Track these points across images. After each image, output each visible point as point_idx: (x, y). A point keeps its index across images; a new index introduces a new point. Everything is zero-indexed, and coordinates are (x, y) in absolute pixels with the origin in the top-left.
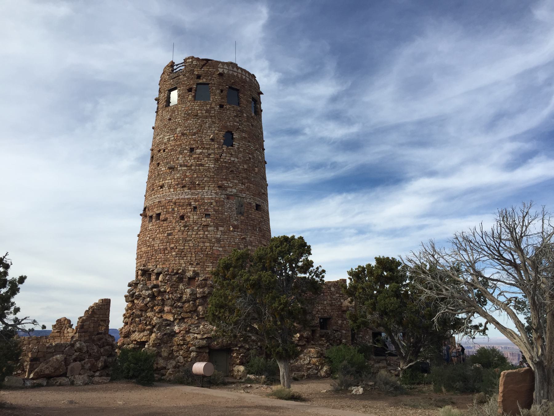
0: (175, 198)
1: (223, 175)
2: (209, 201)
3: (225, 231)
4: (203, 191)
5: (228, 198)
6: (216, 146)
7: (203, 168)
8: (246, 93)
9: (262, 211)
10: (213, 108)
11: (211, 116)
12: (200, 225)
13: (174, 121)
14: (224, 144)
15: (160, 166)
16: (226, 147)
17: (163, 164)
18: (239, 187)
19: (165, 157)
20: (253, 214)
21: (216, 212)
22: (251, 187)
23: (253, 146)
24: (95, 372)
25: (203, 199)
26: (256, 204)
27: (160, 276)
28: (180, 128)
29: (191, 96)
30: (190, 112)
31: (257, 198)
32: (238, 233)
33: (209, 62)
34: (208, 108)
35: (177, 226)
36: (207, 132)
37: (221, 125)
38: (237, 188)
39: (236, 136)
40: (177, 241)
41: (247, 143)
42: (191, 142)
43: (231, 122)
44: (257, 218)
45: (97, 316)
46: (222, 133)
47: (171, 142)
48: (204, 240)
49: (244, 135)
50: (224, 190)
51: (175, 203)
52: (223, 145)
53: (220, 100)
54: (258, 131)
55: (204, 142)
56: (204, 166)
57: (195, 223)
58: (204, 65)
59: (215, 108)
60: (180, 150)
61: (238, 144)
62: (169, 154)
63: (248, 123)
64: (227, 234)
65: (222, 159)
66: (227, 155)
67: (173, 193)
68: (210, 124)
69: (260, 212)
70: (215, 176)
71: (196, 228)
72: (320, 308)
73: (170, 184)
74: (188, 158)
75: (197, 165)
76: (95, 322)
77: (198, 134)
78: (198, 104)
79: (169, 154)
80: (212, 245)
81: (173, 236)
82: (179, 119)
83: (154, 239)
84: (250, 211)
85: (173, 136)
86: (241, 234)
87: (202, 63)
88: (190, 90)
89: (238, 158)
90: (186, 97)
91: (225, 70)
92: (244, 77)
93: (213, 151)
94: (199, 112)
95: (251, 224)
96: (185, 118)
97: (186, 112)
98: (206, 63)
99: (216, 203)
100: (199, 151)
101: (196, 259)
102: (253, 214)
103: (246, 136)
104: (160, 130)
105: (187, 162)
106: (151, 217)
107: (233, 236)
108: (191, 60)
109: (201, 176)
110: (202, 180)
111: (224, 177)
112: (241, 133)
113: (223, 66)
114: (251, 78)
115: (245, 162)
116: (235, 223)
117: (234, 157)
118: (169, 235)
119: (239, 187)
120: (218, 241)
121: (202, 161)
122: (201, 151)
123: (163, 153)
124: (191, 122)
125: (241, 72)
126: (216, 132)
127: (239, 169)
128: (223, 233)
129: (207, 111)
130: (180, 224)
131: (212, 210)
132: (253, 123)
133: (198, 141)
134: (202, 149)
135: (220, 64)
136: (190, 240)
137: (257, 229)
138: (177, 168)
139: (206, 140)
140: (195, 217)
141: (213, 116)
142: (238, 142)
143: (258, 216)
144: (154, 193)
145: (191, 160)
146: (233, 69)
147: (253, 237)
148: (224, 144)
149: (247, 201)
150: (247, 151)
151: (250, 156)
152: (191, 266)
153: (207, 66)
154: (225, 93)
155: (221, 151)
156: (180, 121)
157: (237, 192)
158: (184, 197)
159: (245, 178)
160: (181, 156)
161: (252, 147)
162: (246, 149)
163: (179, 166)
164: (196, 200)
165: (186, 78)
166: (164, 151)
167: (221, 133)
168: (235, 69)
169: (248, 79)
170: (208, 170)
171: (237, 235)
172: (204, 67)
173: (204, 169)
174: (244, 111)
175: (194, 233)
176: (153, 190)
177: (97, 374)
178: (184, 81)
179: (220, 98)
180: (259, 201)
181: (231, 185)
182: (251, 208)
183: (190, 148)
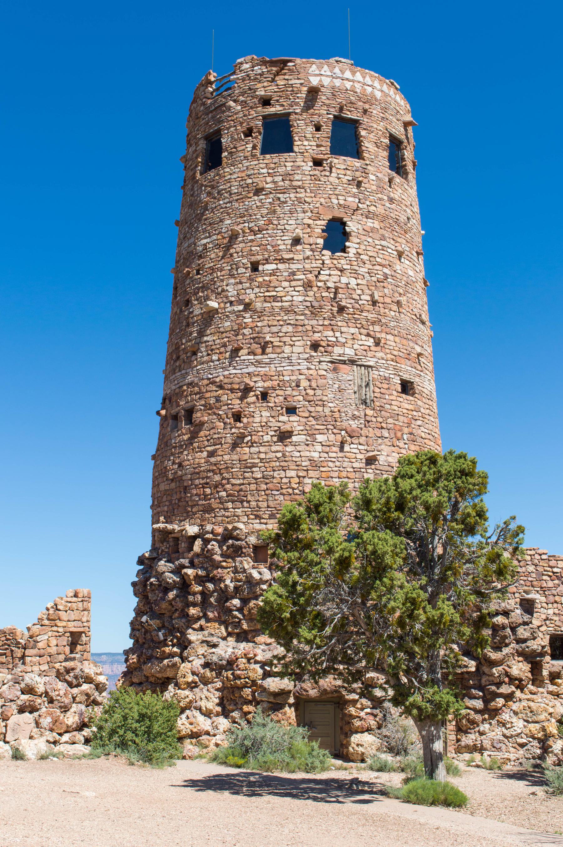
1: (324, 318)
2: (294, 378)
3: (331, 443)
4: (280, 356)
5: (335, 370)
6: (309, 253)
7: (279, 304)
8: (375, 126)
9: (416, 395)
12: (275, 431)
13: (217, 204)
14: (325, 247)
16: (330, 253)
18: (360, 343)
20: (393, 403)
21: (309, 401)
22: (388, 342)
23: (393, 248)
24: (60, 735)
26: (401, 380)
27: (196, 543)
30: (249, 181)
31: (403, 366)
32: (360, 447)
33: (290, 64)
35: (228, 435)
38: (356, 347)
39: (352, 226)
41: (377, 242)
42: (253, 249)
43: (340, 197)
44: (405, 411)
45: (64, 624)
48: (286, 464)
49: (372, 225)
50: (326, 352)
51: (221, 387)
52: (323, 249)
54: (405, 211)
55: (281, 247)
56: (282, 301)
57: (265, 426)
59: (304, 168)
61: (357, 246)
63: (380, 196)
64: (334, 449)
65: (320, 281)
66: (332, 273)
67: (218, 363)
68: (292, 205)
69: (411, 398)
70: (306, 322)
71: (267, 438)
72: (551, 612)
73: (210, 343)
74: (248, 285)
76: (60, 636)
77: (267, 229)
78: (265, 161)
80: (301, 474)
81: (219, 458)
84: (387, 397)
86: (366, 447)
88: (249, 133)
89: (356, 279)
90: (239, 149)
91: (323, 78)
92: (369, 89)
93: (300, 266)
94: (269, 179)
95: (391, 426)
98: (282, 69)
99: (309, 380)
101: (268, 507)
102: (393, 403)
103: (377, 225)
106: (175, 418)
107: (348, 454)
109: (275, 323)
110: (278, 333)
111: (326, 322)
112: (365, 220)
114: (387, 91)
116: (354, 424)
117: (349, 275)
118: (212, 454)
119: (360, 343)
121: (276, 289)
122: (273, 266)
125: (361, 79)
127: (360, 302)
129: (287, 176)
130: (233, 430)
131: (301, 398)
132: (392, 195)
134: (275, 262)
135: (314, 66)
136: (254, 465)
137: (405, 437)
139: (284, 243)
140: (265, 414)
142: (358, 241)
143: (407, 406)
144: (180, 366)
145: (253, 289)
146: (342, 72)
147: (394, 454)
148: (325, 247)
149: (381, 373)
150: (378, 260)
151: (386, 270)
152: (258, 521)
153: (285, 74)
154: (327, 129)
155: (315, 265)
157: (356, 355)
158: (239, 371)
159: (373, 323)
160: (232, 281)
161: (390, 250)
162: (375, 254)
163: (228, 305)
164: (266, 377)
165: (239, 108)
167: (319, 222)
168: (348, 74)
169: (378, 95)
171: (358, 451)
172: (277, 78)
173: (282, 308)
174: (369, 167)
175: (262, 449)
177: (66, 737)
178: (236, 114)
179: (315, 144)
181: (344, 340)
182: (389, 388)
183: (251, 263)
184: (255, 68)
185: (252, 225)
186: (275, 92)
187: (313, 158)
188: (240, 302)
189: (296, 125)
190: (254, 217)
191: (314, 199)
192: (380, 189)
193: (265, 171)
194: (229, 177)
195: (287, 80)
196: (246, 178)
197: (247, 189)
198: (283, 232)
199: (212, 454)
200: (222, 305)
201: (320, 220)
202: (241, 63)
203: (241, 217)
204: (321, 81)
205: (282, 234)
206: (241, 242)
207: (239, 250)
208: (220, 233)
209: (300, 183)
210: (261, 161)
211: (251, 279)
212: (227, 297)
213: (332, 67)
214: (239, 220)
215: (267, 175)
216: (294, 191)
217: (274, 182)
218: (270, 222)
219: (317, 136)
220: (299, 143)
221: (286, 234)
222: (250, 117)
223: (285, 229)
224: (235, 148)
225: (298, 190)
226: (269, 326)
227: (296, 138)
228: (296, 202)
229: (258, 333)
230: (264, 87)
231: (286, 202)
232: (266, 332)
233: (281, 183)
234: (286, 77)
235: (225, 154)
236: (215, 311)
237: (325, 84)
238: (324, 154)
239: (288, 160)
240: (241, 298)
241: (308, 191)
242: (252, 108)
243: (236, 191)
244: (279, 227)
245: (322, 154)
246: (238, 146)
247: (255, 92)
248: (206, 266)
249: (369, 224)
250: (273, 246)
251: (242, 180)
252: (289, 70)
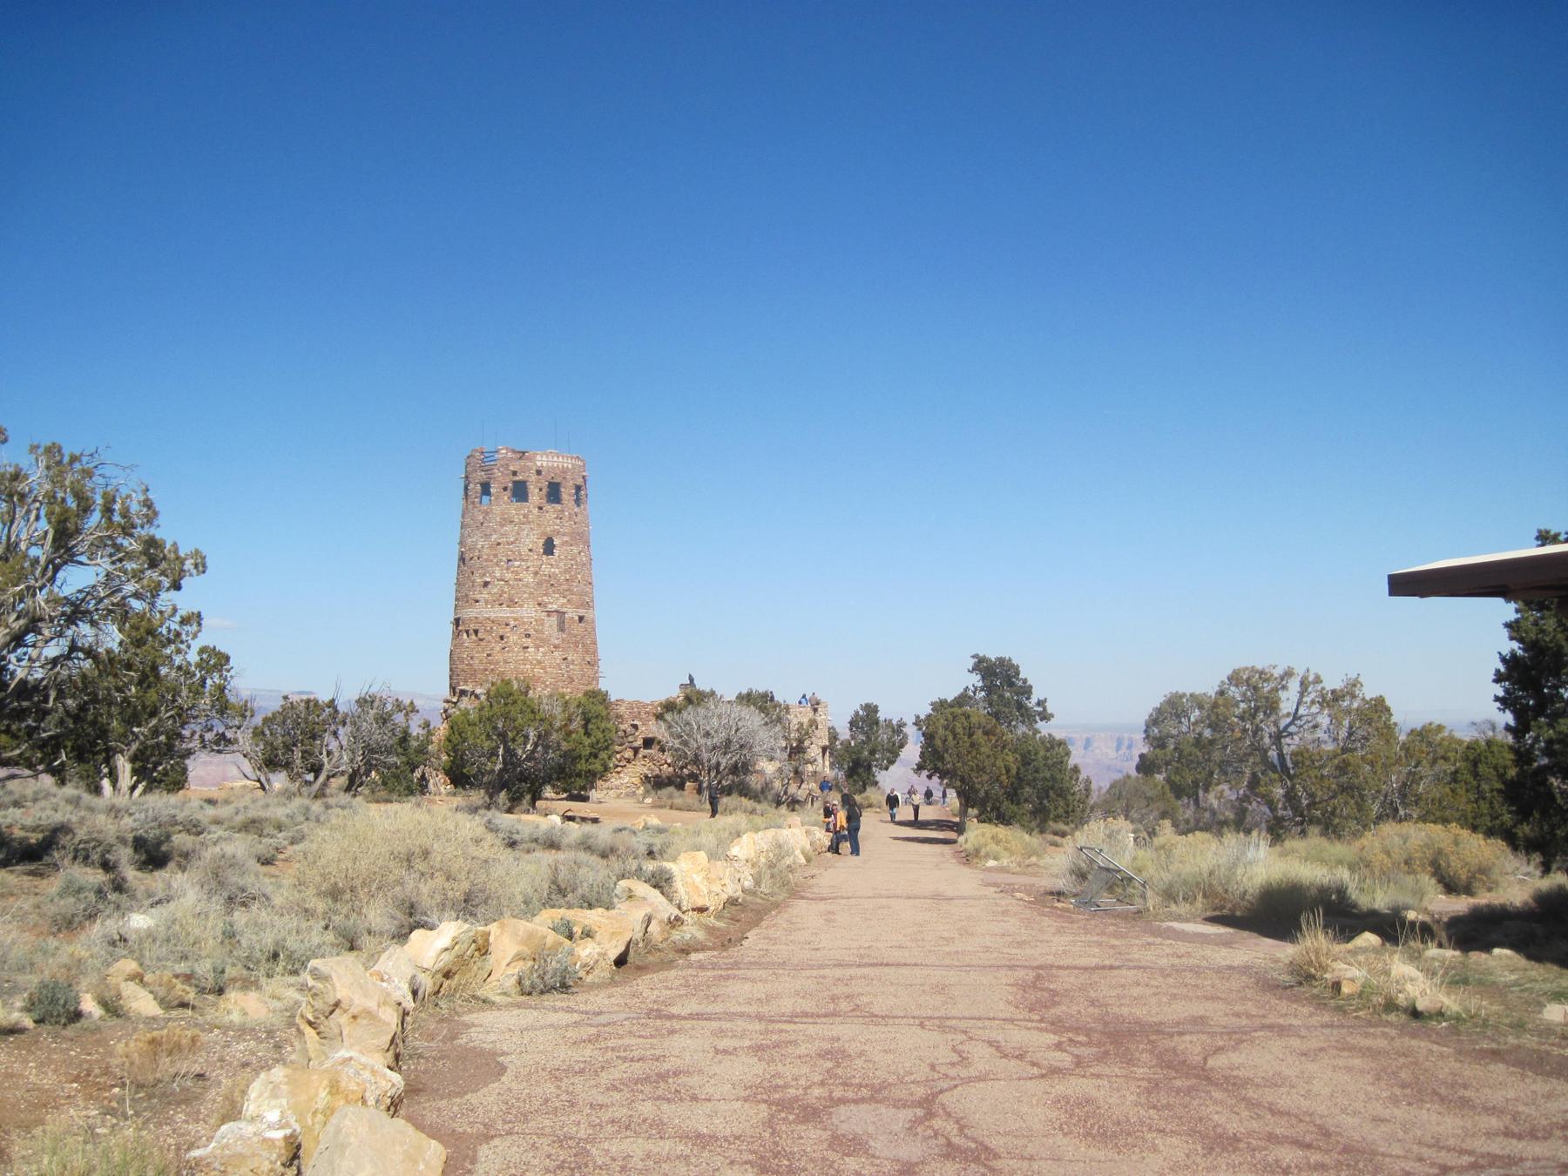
0: (493, 615)
5: (548, 616)
25: (522, 618)
39: (556, 542)
40: (498, 663)
46: (542, 542)
51: (493, 622)
57: (515, 644)
58: (520, 458)
75: (516, 580)
83: (472, 658)
88: (505, 489)
92: (565, 465)
100: (517, 563)
115: (566, 571)
118: (489, 655)
120: (539, 662)
128: (544, 654)
129: (525, 516)
139: (524, 550)
154: (545, 490)
164: (515, 619)
168: (555, 459)
169: (570, 466)
170: (527, 586)
176: (467, 602)
180: (582, 612)
188: (503, 580)
192: (570, 518)
199: (489, 655)
211: (508, 569)
213: (547, 457)
242: (507, 475)
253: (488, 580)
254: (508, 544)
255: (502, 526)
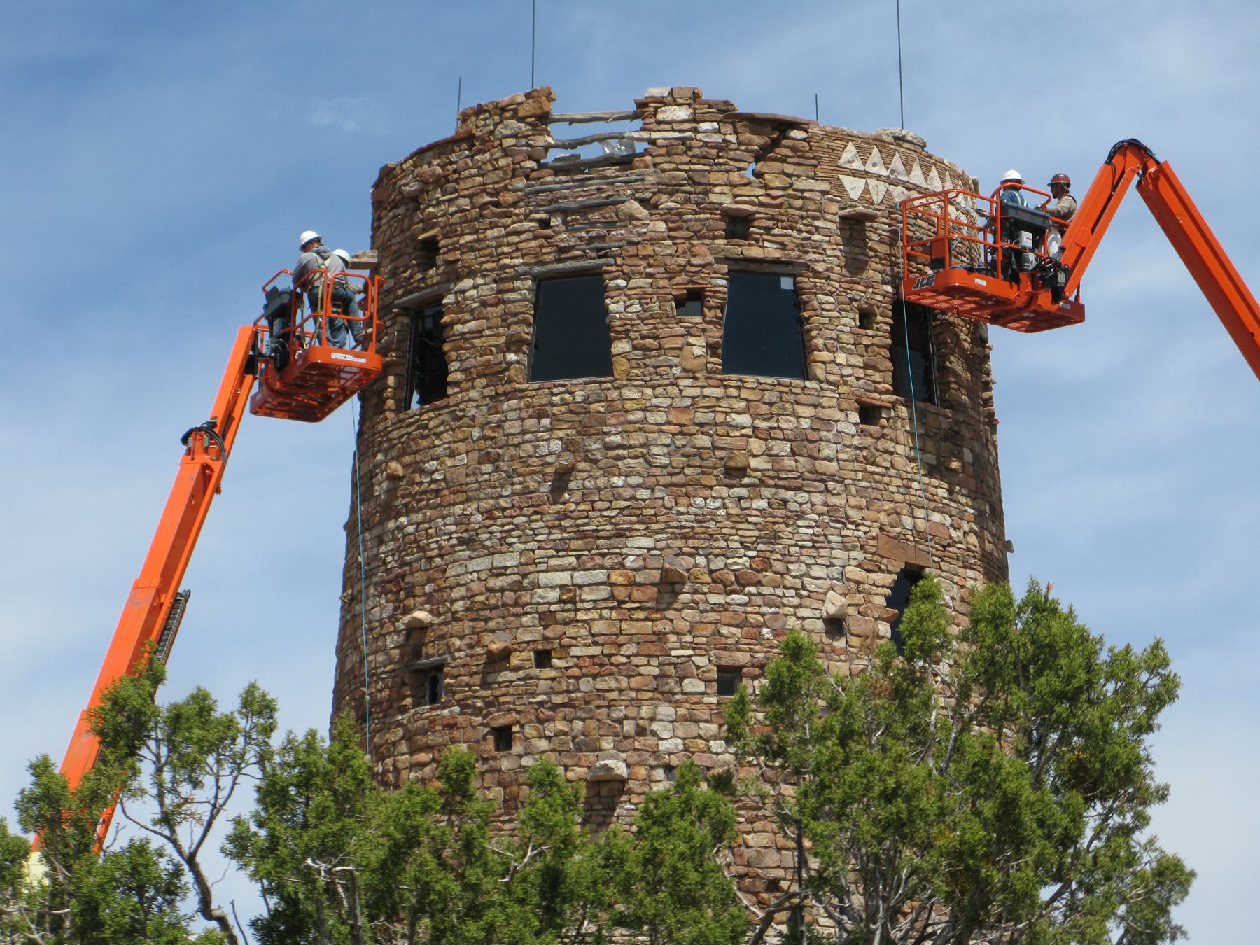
10: (827, 422)
11: (823, 478)
13: (601, 482)
15: (517, 748)
17: (543, 744)
19: (558, 700)
28: (650, 533)
29: (701, 341)
30: (704, 441)
33: (796, 134)
34: (805, 424)
36: (807, 575)
37: (875, 531)
42: (724, 630)
47: (594, 615)
53: (860, 373)
59: (841, 427)
60: (656, 671)
62: (585, 684)
77: (758, 584)
78: (744, 394)
79: (585, 684)
82: (634, 480)
85: (600, 575)
87: (758, 140)
90: (668, 344)
91: (872, 182)
94: (756, 445)
96: (675, 479)
97: (681, 441)
98: (775, 143)
104: (489, 514)
105: (709, 750)
108: (682, 113)
112: (961, 571)
113: (864, 163)
123: (535, 672)
124: (712, 504)
126: (854, 572)
129: (802, 444)
133: (765, 625)
135: (850, 146)
138: (649, 781)
141: (833, 477)
153: (783, 160)
156: (643, 494)
160: (666, 710)
163: (659, 774)
165: (661, 226)
166: (543, 659)
167: (877, 577)
178: (653, 241)
179: (858, 361)
183: (721, 669)
184: (704, 126)
185: (718, 563)
186: (762, 205)
187: (858, 401)
189: (815, 303)
190: (723, 544)
191: (866, 513)
193: (744, 420)
194: (640, 415)
195: (789, 176)
196: (694, 429)
197: (697, 462)
198: (801, 597)
200: (642, 772)
201: (882, 571)
202: (662, 102)
203: (685, 537)
204: (866, 190)
205: (796, 601)
206: (686, 606)
207: (684, 626)
208: (622, 566)
209: (833, 467)
210: (734, 392)
212: (655, 753)
214: (679, 543)
215: (749, 431)
216: (822, 486)
217: (769, 454)
218: (767, 564)
219: (866, 341)
220: (826, 355)
221: (807, 602)
222: (695, 261)
223: (804, 588)
224: (656, 338)
225: (831, 485)
226: (779, 849)
227: (819, 342)
228: (826, 519)
229: (749, 864)
230: (733, 185)
231: (800, 515)
232: (771, 863)
233: (789, 462)
234: (789, 169)
235: (620, 347)
236: (617, 786)
237: (877, 199)
238: (882, 393)
239: (803, 398)
240: (697, 759)
241: (853, 490)
242: (697, 235)
243: (666, 461)
244: (789, 580)
245: (876, 391)
246: (663, 331)
247: (706, 193)
248: (575, 651)
249: (970, 583)
250: (776, 633)
251: (681, 433)
252: (794, 149)
253: (621, 769)
254: (717, 580)
255: (685, 489)
